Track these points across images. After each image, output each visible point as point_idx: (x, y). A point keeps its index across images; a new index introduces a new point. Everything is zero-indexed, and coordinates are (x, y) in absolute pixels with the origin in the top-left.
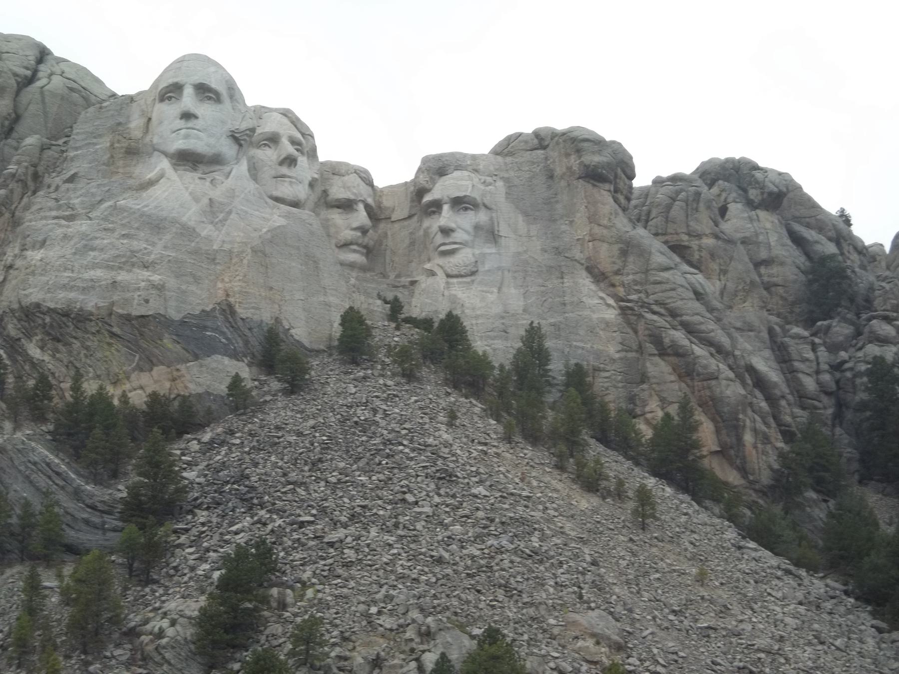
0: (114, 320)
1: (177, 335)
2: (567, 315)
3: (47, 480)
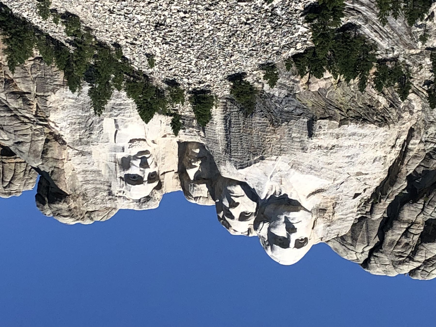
1: (304, 108)
3: (382, 28)
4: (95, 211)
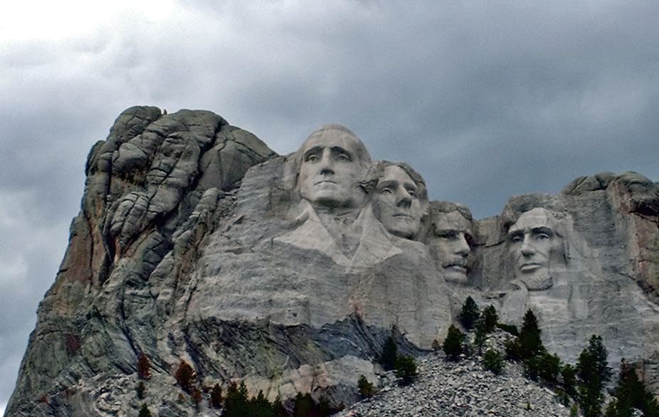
0: (270, 330)
1: (317, 340)
2: (623, 320)
4: (594, 190)
